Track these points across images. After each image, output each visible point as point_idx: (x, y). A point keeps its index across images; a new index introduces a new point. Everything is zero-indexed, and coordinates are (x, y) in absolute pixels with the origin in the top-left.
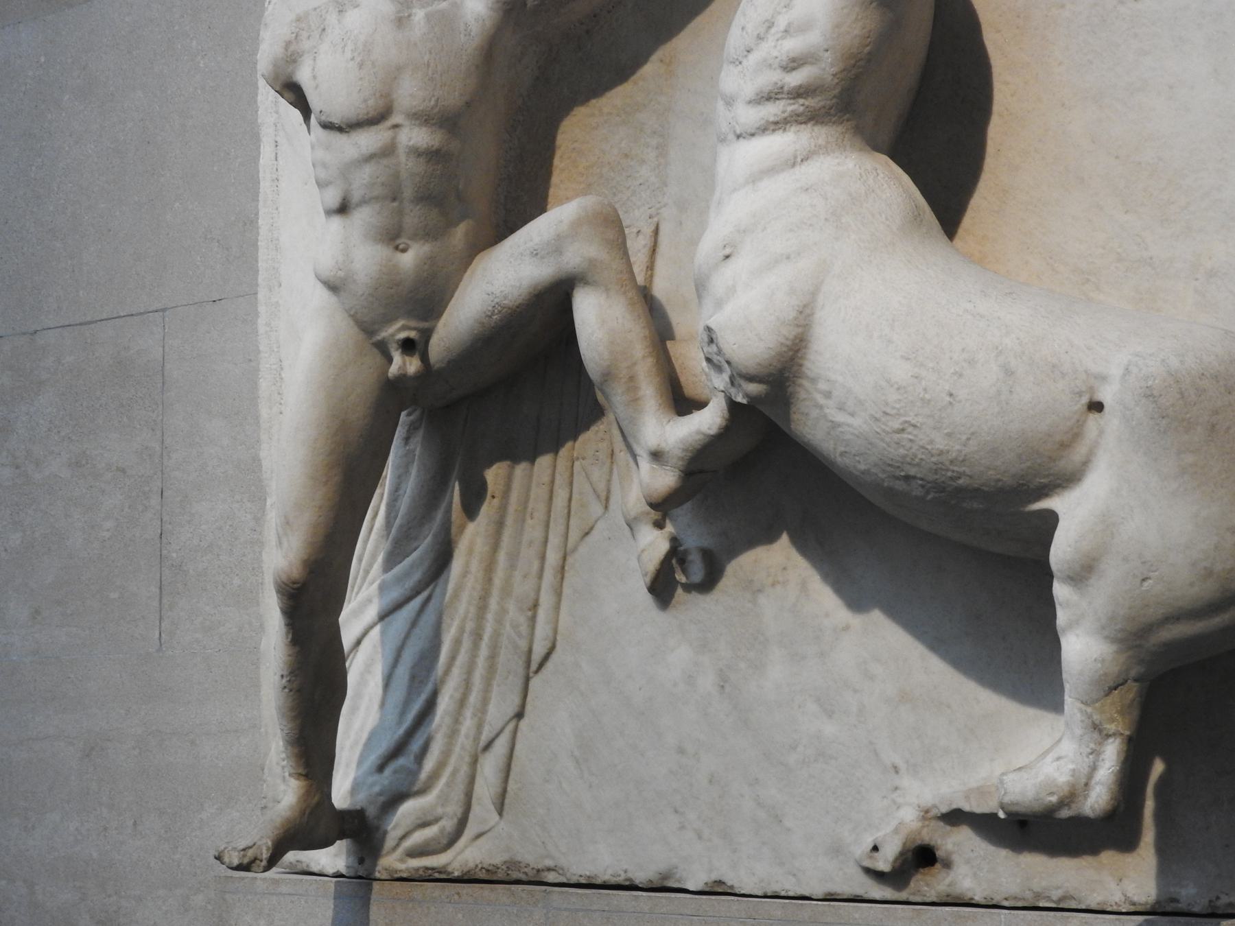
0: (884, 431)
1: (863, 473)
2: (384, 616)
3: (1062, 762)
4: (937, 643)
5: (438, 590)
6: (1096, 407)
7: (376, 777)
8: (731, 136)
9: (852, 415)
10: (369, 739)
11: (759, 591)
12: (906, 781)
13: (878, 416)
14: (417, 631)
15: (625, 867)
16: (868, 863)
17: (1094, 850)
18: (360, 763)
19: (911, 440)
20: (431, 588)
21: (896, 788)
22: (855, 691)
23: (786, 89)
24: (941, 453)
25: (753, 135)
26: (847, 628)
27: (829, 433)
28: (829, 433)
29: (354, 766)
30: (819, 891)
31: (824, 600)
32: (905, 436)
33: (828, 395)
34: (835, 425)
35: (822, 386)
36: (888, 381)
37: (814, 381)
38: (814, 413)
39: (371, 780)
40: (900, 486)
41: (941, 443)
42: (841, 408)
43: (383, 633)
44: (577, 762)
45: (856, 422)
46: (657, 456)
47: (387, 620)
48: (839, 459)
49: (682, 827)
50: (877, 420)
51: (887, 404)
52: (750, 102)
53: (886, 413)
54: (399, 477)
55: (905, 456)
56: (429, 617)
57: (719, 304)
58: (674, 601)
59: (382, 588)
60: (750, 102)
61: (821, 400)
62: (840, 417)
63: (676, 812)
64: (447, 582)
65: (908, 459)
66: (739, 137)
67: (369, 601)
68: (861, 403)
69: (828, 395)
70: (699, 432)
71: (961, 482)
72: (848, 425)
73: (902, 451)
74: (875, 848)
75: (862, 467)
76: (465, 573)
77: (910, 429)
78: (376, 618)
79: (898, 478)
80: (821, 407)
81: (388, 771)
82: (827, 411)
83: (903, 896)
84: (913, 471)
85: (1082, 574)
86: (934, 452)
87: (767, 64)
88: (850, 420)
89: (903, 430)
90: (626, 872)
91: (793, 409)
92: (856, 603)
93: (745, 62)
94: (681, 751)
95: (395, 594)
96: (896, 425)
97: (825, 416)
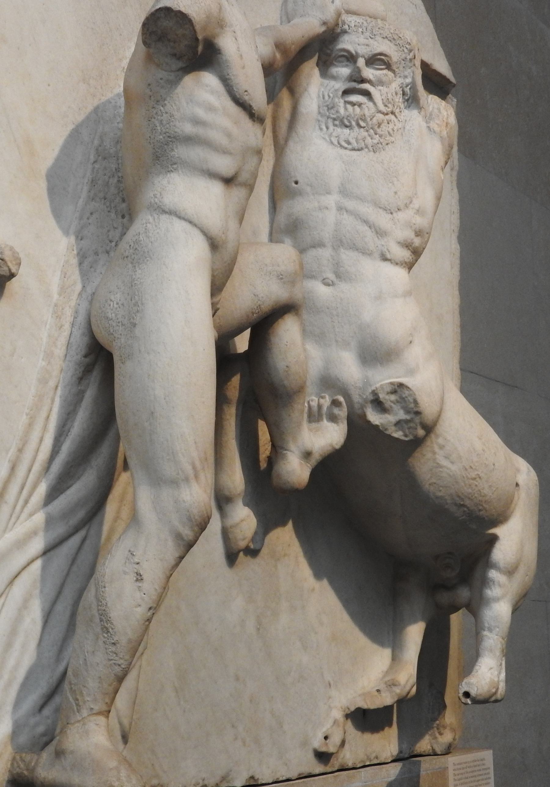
0: (467, 477)
1: (437, 497)
2: (46, 552)
3: (492, 670)
4: (346, 603)
5: (92, 532)
6: (517, 485)
7: (38, 718)
8: (377, 255)
9: (452, 463)
10: (27, 678)
11: (279, 559)
12: (333, 693)
13: (467, 467)
14: (75, 568)
15: (204, 776)
16: (323, 749)
17: (383, 729)
18: (17, 704)
19: (476, 485)
20: (86, 528)
21: (330, 698)
22: (316, 633)
23: (413, 246)
24: (485, 496)
25: (397, 264)
26: (313, 590)
27: (431, 470)
28: (431, 470)
29: (9, 708)
30: (294, 775)
31: (305, 571)
32: (475, 482)
33: (442, 447)
34: (439, 466)
35: (440, 441)
36: (474, 449)
37: (437, 436)
38: (429, 455)
39: (32, 721)
40: (453, 509)
41: (486, 491)
42: (447, 457)
43: (44, 568)
44: (177, 692)
45: (454, 468)
46: (307, 455)
47: (48, 555)
48: (427, 486)
49: (236, 739)
50: (466, 469)
51: (473, 462)
52: (399, 243)
53: (471, 467)
54: (69, 414)
55: (470, 493)
56: (86, 556)
57: (411, 372)
58: (237, 562)
59: (49, 522)
60: (399, 243)
61: (437, 449)
62: (444, 463)
63: (233, 726)
64: (101, 524)
65: (470, 496)
66: (385, 259)
67: (35, 533)
68: (460, 457)
69: (442, 447)
70: (331, 445)
71: (481, 513)
72: (447, 469)
73: (470, 491)
74: (326, 738)
75: (440, 494)
76: (116, 518)
77: (478, 479)
78: (41, 553)
79: (456, 504)
80: (434, 453)
81: (47, 711)
82: (437, 456)
83: (328, 769)
84: (467, 502)
85: (510, 572)
86: (483, 494)
87: (409, 225)
88: (450, 465)
89: (474, 479)
90: (203, 780)
91: (418, 450)
92: (318, 575)
93: (395, 214)
94: (237, 679)
95: (60, 530)
96: (473, 475)
97: (435, 460)
